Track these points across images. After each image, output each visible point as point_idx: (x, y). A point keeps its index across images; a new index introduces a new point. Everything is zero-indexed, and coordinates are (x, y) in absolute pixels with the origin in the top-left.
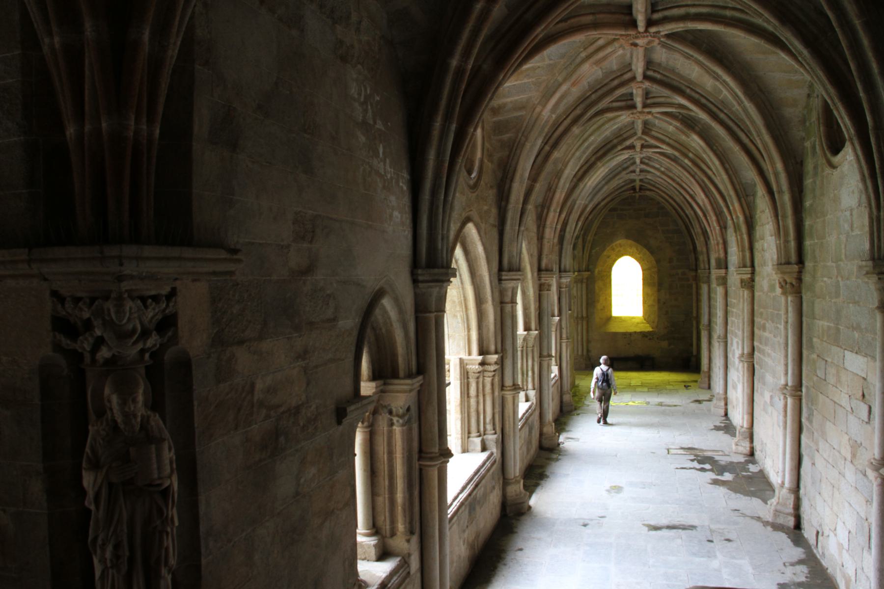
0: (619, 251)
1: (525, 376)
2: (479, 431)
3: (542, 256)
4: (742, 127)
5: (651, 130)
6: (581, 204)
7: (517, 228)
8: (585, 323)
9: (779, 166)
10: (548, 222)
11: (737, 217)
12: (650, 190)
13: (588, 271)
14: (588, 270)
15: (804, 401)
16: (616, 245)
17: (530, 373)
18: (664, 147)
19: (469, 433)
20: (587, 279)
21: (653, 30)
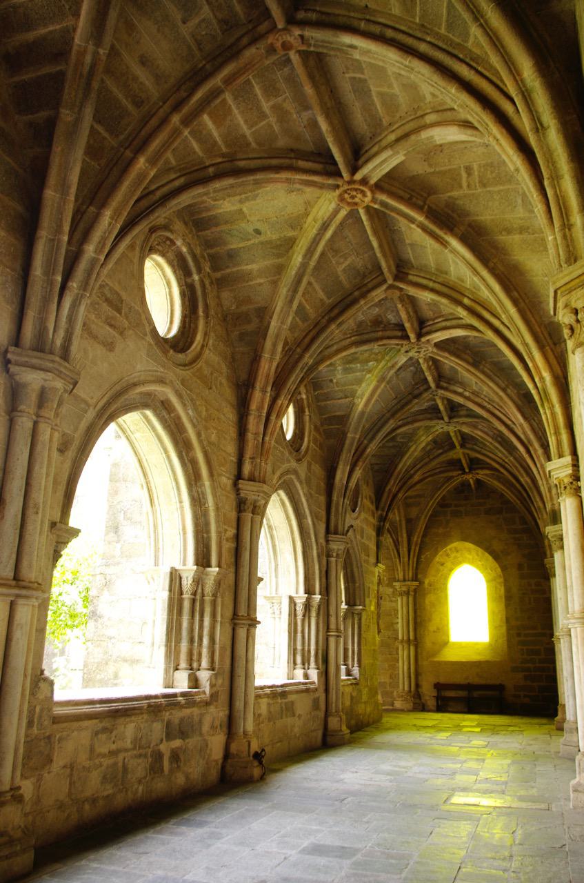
0: (455, 557)
3: (244, 458)
4: (461, 56)
5: (408, 274)
6: (354, 439)
7: (59, 278)
8: (412, 648)
11: (542, 379)
13: (416, 581)
14: (415, 578)
16: (450, 549)
17: (206, 641)
20: (415, 591)
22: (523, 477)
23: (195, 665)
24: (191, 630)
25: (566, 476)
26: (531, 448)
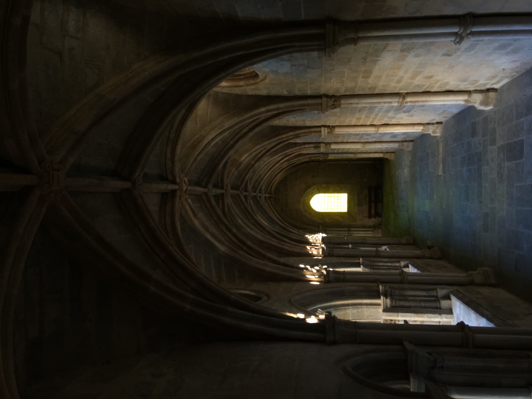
1: (391, 267)
2: (435, 301)
9: (263, 109)
10: (291, 249)
11: (291, 136)
12: (271, 188)
15: (408, 91)
16: (304, 209)
17: (389, 264)
18: (247, 178)
19: (437, 308)
21: (178, 180)
22: (284, 166)
23: (399, 268)
24: (385, 269)
25: (328, 130)
26: (288, 154)
